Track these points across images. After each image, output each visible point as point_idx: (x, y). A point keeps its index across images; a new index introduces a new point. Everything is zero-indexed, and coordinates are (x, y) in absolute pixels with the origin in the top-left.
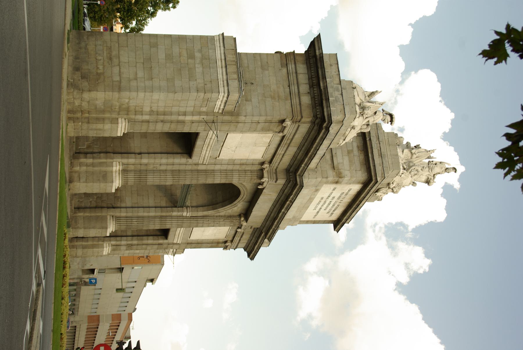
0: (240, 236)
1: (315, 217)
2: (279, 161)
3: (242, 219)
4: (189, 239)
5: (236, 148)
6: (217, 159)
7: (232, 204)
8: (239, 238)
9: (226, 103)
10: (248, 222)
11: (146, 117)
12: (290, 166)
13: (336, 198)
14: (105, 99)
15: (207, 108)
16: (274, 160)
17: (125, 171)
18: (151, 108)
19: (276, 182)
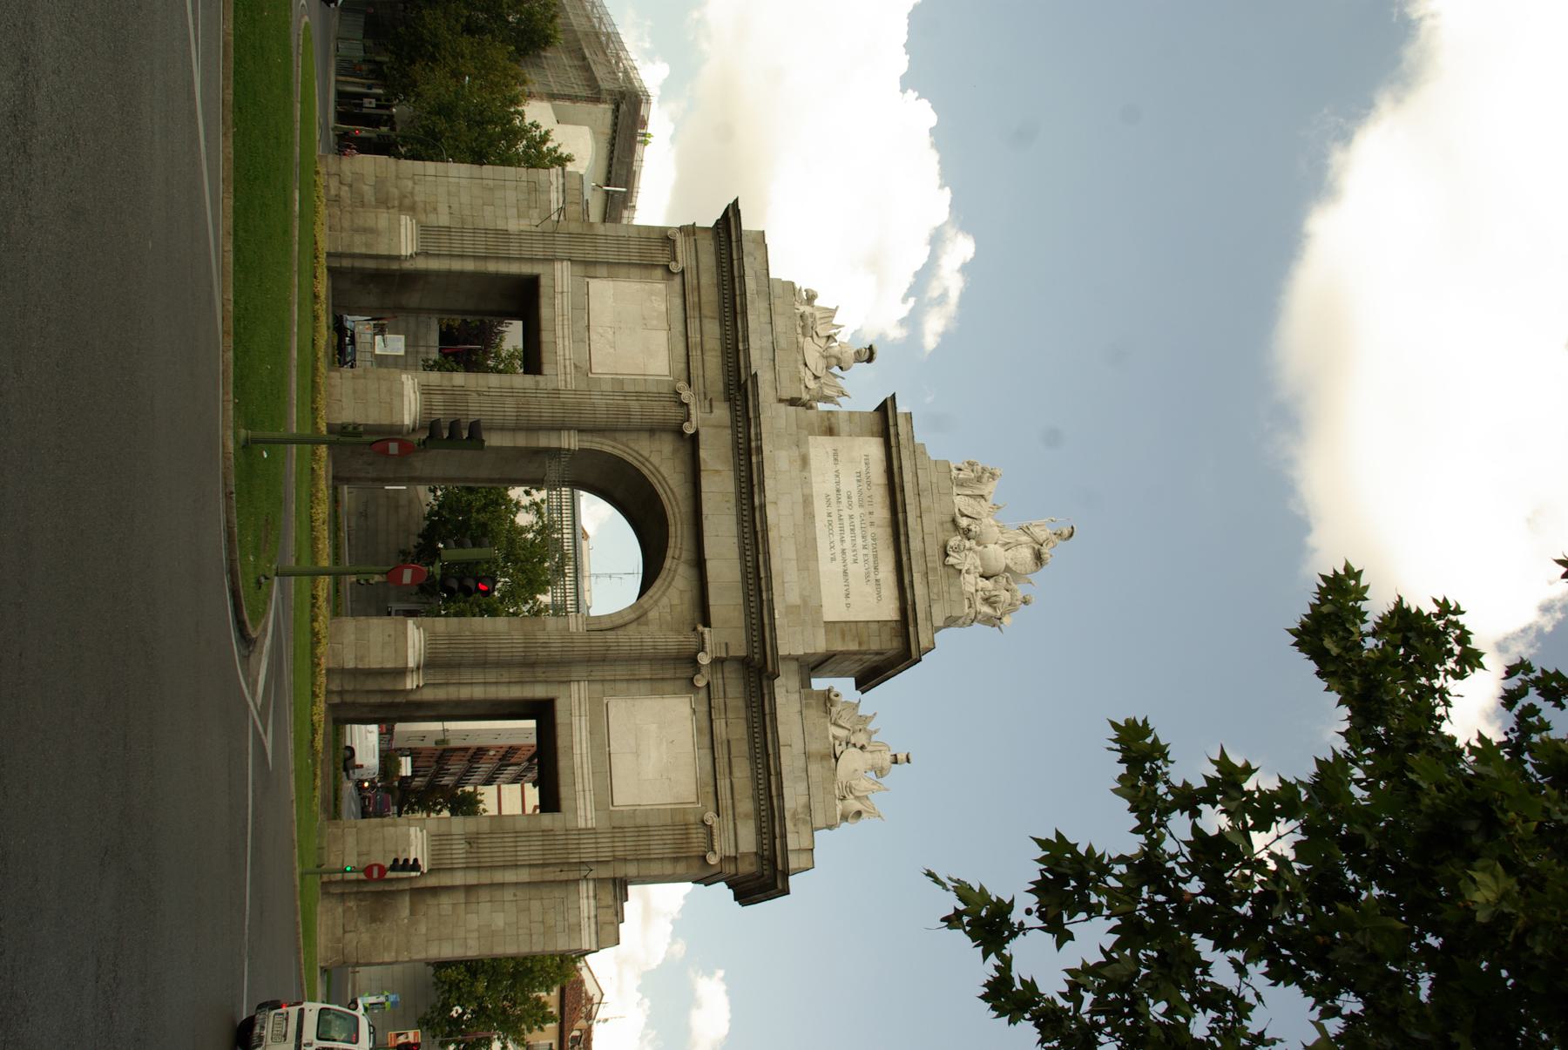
0: (727, 771)
1: (849, 601)
2: (702, 373)
3: (700, 628)
4: (611, 808)
5: (614, 333)
6: (590, 375)
7: (663, 574)
8: (728, 781)
9: (564, 191)
10: (713, 626)
11: (444, 220)
12: (727, 386)
13: (855, 499)
14: (376, 177)
15: (538, 210)
16: (691, 371)
17: (426, 391)
18: (450, 207)
19: (711, 412)
